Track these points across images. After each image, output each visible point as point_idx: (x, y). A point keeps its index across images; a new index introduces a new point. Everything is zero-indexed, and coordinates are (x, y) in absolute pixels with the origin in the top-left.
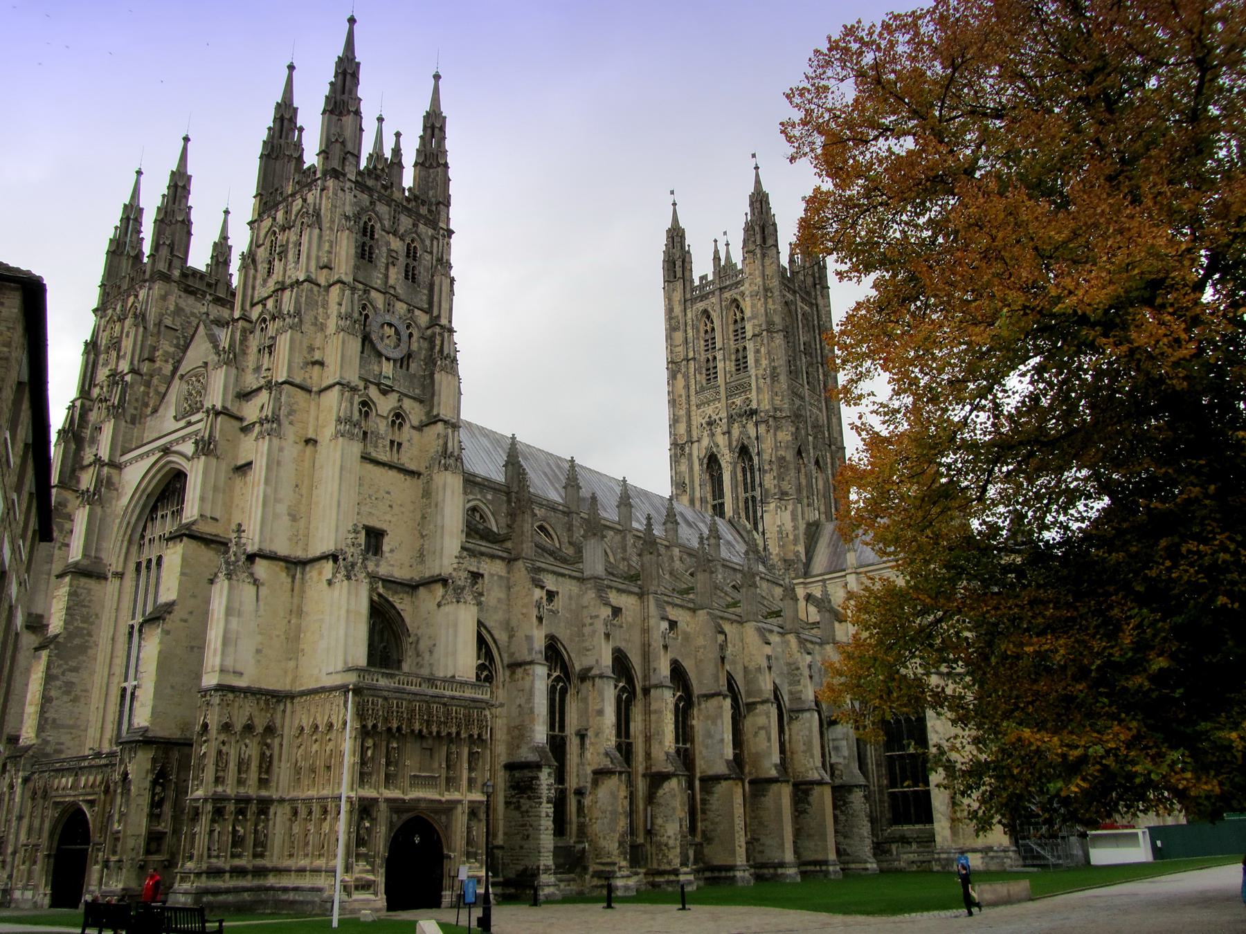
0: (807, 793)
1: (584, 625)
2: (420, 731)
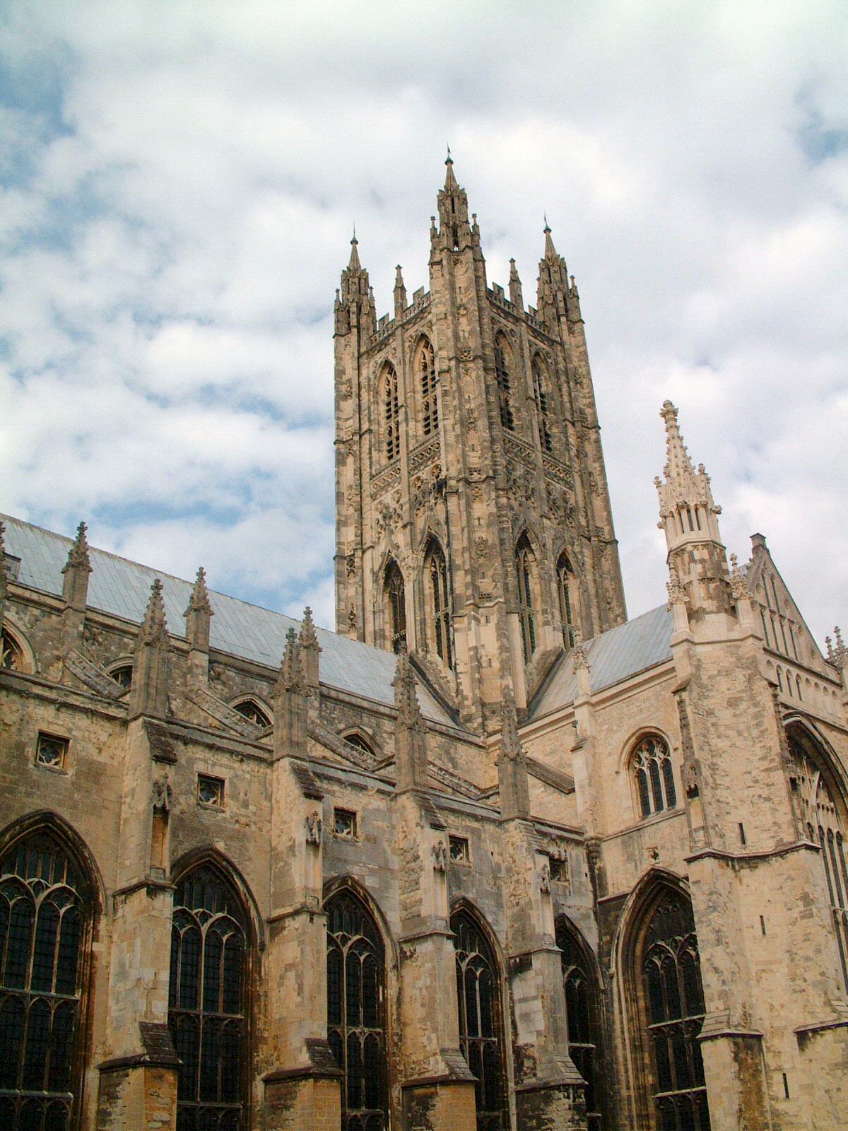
0: (425, 1103)
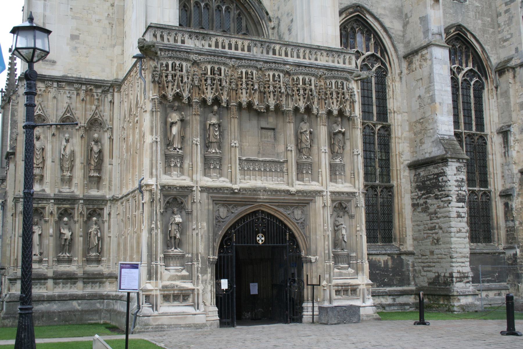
1: (499, 15)
2: (250, 105)
